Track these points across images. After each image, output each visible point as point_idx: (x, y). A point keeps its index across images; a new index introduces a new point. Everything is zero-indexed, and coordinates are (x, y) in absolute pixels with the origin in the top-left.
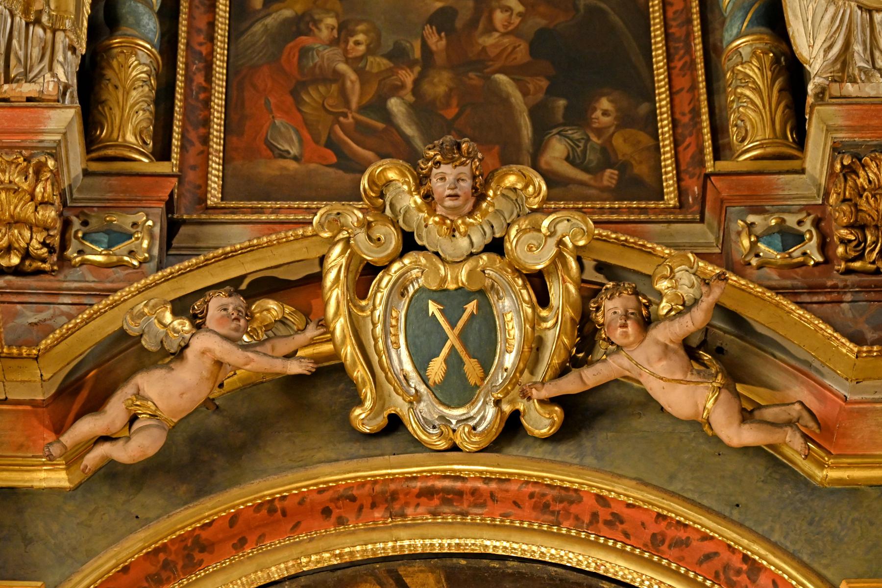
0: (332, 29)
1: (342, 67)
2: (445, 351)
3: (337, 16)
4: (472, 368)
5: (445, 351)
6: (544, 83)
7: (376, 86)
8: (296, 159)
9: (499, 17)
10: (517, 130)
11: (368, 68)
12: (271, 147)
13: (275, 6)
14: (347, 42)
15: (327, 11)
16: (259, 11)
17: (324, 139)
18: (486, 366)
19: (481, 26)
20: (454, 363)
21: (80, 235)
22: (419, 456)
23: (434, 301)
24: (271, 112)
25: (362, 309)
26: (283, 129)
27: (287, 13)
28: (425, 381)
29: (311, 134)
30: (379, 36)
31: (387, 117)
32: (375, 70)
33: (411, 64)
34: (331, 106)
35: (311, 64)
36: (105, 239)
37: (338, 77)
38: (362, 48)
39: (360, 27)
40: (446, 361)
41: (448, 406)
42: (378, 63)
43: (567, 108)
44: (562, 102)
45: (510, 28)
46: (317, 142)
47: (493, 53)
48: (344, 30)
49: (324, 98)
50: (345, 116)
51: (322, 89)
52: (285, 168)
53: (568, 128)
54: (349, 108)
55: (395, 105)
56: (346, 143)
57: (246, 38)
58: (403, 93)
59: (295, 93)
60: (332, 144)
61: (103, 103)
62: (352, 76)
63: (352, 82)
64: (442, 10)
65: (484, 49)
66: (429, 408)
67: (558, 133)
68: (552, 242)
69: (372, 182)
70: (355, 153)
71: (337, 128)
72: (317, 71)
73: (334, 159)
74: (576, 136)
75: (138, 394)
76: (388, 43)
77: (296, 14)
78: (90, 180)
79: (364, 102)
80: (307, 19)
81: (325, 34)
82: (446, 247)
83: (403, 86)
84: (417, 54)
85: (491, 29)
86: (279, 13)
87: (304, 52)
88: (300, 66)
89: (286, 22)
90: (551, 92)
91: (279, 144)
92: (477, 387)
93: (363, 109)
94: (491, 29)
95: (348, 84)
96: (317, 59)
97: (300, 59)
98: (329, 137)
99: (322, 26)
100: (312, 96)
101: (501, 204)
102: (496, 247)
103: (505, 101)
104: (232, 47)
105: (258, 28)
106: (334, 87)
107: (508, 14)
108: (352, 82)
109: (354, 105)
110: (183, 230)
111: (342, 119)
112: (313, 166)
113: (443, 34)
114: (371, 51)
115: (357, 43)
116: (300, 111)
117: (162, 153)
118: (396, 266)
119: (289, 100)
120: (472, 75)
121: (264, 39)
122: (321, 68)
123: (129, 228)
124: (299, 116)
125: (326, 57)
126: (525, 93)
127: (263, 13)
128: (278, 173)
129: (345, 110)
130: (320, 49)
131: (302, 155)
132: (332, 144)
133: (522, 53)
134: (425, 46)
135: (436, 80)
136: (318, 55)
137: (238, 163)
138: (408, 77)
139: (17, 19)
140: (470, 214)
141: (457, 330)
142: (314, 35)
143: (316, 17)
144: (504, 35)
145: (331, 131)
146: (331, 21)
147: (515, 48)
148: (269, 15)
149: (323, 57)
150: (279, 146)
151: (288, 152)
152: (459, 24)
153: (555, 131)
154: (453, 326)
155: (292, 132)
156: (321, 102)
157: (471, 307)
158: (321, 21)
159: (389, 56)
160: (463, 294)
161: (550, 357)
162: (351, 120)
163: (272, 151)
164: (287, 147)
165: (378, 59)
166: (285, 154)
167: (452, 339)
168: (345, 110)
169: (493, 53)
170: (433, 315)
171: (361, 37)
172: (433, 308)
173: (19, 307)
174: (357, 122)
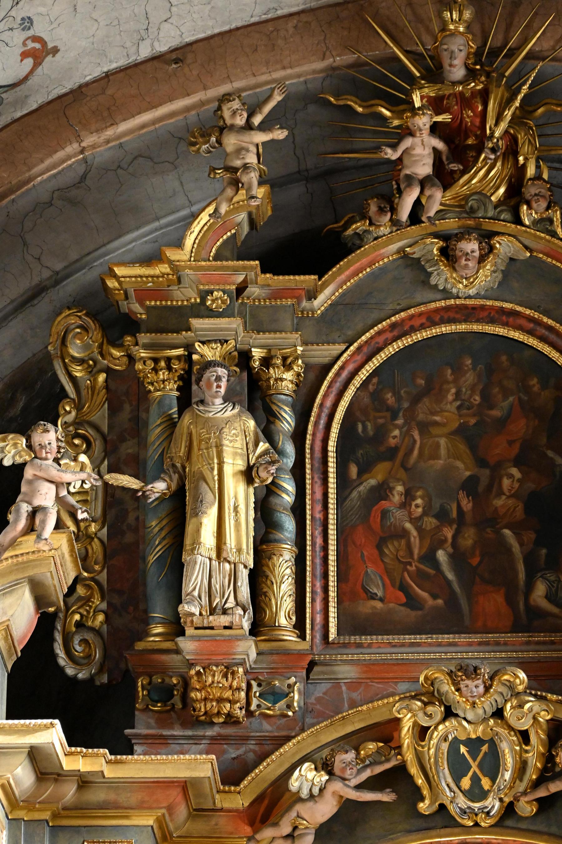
0: (401, 495)
1: (408, 525)
2: (470, 774)
3: (404, 484)
4: (486, 783)
5: (470, 774)
6: (533, 536)
7: (429, 541)
8: (381, 600)
9: (506, 482)
10: (516, 576)
11: (424, 527)
12: (366, 591)
13: (365, 476)
14: (410, 505)
15: (398, 480)
16: (355, 480)
17: (398, 584)
18: (493, 780)
19: (494, 490)
20: (475, 780)
21: (258, 694)
22: (456, 830)
23: (463, 745)
24: (365, 563)
25: (423, 747)
26: (373, 577)
27: (373, 482)
28: (459, 788)
29: (390, 580)
30: (430, 500)
31: (436, 564)
32: (428, 528)
33: (450, 523)
34: (402, 557)
35: (389, 524)
36: (271, 698)
37: (405, 534)
38: (420, 510)
39: (419, 493)
40: (471, 779)
41: (473, 801)
42: (430, 522)
43: (547, 555)
44: (544, 551)
45: (513, 492)
46: (393, 585)
47: (502, 511)
48: (409, 495)
49: (398, 551)
50: (411, 565)
51: (396, 543)
52: (375, 607)
53: (547, 572)
54: (413, 559)
55: (441, 555)
56: (411, 587)
57: (348, 503)
58: (446, 545)
59: (379, 547)
60: (403, 588)
61: (265, 594)
62: (414, 533)
63: (415, 537)
64: (470, 478)
65: (496, 508)
66: (463, 802)
67: (541, 577)
68: (530, 716)
69: (426, 678)
70: (417, 595)
71: (406, 575)
72: (392, 528)
73: (404, 600)
74: (552, 578)
75: (298, 816)
76: (437, 505)
77: (379, 483)
78: (261, 657)
79: (422, 553)
80: (386, 487)
81: (396, 499)
82: (470, 717)
83: (446, 540)
84: (454, 514)
85: (501, 493)
86: (368, 481)
87: (385, 514)
88: (382, 526)
89: (373, 489)
90: (538, 543)
91: (371, 588)
92: (489, 791)
93: (423, 559)
94: (501, 493)
95: (412, 539)
96: (392, 520)
97: (382, 520)
98: (401, 582)
99: (395, 493)
100: (390, 549)
101: (501, 689)
102: (499, 714)
103: (508, 550)
104: (339, 511)
105: (355, 494)
106: (403, 542)
107: (511, 480)
108: (415, 537)
109: (416, 557)
110: (316, 669)
111: (408, 567)
112: (391, 605)
113: (470, 498)
114: (425, 513)
115: (417, 506)
116: (383, 561)
117: (302, 636)
118: (441, 727)
119: (376, 552)
120: (489, 530)
121: (359, 503)
122: (395, 526)
123: (286, 689)
124: (382, 566)
125: (398, 517)
126: (521, 545)
127: (357, 483)
128: (370, 611)
129: (410, 560)
130: (394, 511)
131: (384, 597)
132: (403, 588)
133: (519, 513)
134: (459, 507)
135: (466, 535)
136: (393, 516)
137: (346, 604)
138: (449, 533)
139: (214, 562)
140: (483, 696)
141: (477, 763)
142: (390, 500)
143: (391, 485)
144: (509, 497)
145: (402, 578)
146: (400, 488)
147: (515, 508)
148: (362, 483)
149: (396, 519)
150: (371, 590)
151: (376, 594)
152: (481, 489)
153: (539, 575)
154: (474, 760)
155: (378, 578)
156: (395, 554)
157: (485, 748)
158: (393, 488)
159: (436, 516)
160: (479, 741)
161: (532, 775)
162: (414, 568)
163: (366, 593)
164: (375, 591)
165: (430, 519)
166: (374, 596)
167: (474, 767)
168: (410, 560)
169: (502, 511)
170: (463, 753)
171: (419, 501)
172: (463, 749)
173: (225, 746)
174: (418, 569)
